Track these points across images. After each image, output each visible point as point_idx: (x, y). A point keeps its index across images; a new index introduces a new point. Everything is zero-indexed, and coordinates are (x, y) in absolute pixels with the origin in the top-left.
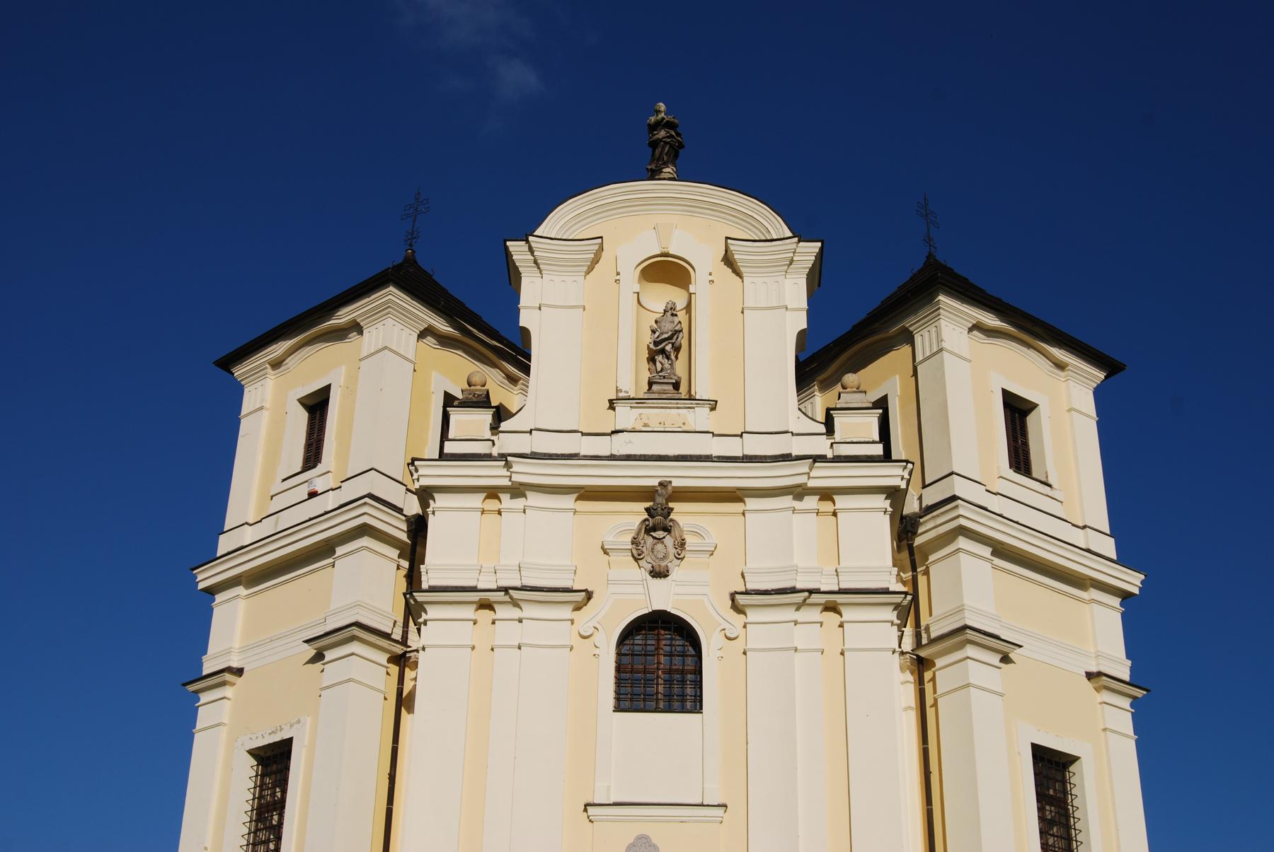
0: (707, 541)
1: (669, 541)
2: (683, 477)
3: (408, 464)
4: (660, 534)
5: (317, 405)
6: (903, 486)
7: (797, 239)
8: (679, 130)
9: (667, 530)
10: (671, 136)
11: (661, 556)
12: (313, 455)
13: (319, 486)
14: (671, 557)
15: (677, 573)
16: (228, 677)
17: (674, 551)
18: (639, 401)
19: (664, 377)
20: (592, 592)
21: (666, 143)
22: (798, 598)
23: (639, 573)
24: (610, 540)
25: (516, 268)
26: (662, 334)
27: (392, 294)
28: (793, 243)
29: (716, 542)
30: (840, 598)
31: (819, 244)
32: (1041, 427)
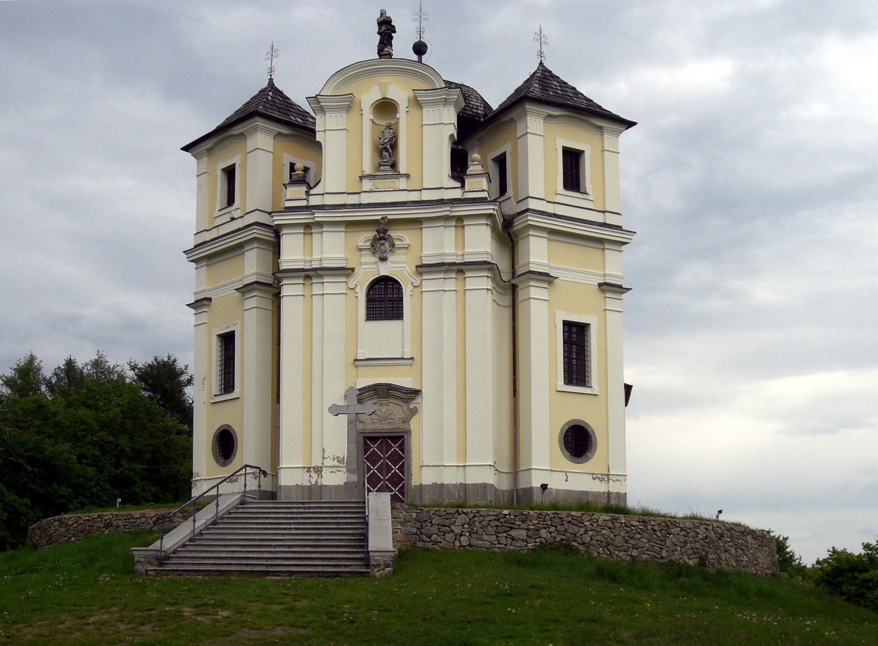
0: (405, 243)
1: (387, 245)
2: (393, 214)
4: (382, 242)
5: (230, 173)
8: (392, 24)
10: (389, 29)
12: (231, 200)
13: (236, 214)
14: (388, 251)
15: (391, 258)
16: (205, 302)
17: (390, 248)
19: (386, 162)
21: (385, 33)
22: (445, 268)
23: (373, 259)
24: (361, 244)
26: (384, 140)
27: (259, 122)
30: (463, 267)
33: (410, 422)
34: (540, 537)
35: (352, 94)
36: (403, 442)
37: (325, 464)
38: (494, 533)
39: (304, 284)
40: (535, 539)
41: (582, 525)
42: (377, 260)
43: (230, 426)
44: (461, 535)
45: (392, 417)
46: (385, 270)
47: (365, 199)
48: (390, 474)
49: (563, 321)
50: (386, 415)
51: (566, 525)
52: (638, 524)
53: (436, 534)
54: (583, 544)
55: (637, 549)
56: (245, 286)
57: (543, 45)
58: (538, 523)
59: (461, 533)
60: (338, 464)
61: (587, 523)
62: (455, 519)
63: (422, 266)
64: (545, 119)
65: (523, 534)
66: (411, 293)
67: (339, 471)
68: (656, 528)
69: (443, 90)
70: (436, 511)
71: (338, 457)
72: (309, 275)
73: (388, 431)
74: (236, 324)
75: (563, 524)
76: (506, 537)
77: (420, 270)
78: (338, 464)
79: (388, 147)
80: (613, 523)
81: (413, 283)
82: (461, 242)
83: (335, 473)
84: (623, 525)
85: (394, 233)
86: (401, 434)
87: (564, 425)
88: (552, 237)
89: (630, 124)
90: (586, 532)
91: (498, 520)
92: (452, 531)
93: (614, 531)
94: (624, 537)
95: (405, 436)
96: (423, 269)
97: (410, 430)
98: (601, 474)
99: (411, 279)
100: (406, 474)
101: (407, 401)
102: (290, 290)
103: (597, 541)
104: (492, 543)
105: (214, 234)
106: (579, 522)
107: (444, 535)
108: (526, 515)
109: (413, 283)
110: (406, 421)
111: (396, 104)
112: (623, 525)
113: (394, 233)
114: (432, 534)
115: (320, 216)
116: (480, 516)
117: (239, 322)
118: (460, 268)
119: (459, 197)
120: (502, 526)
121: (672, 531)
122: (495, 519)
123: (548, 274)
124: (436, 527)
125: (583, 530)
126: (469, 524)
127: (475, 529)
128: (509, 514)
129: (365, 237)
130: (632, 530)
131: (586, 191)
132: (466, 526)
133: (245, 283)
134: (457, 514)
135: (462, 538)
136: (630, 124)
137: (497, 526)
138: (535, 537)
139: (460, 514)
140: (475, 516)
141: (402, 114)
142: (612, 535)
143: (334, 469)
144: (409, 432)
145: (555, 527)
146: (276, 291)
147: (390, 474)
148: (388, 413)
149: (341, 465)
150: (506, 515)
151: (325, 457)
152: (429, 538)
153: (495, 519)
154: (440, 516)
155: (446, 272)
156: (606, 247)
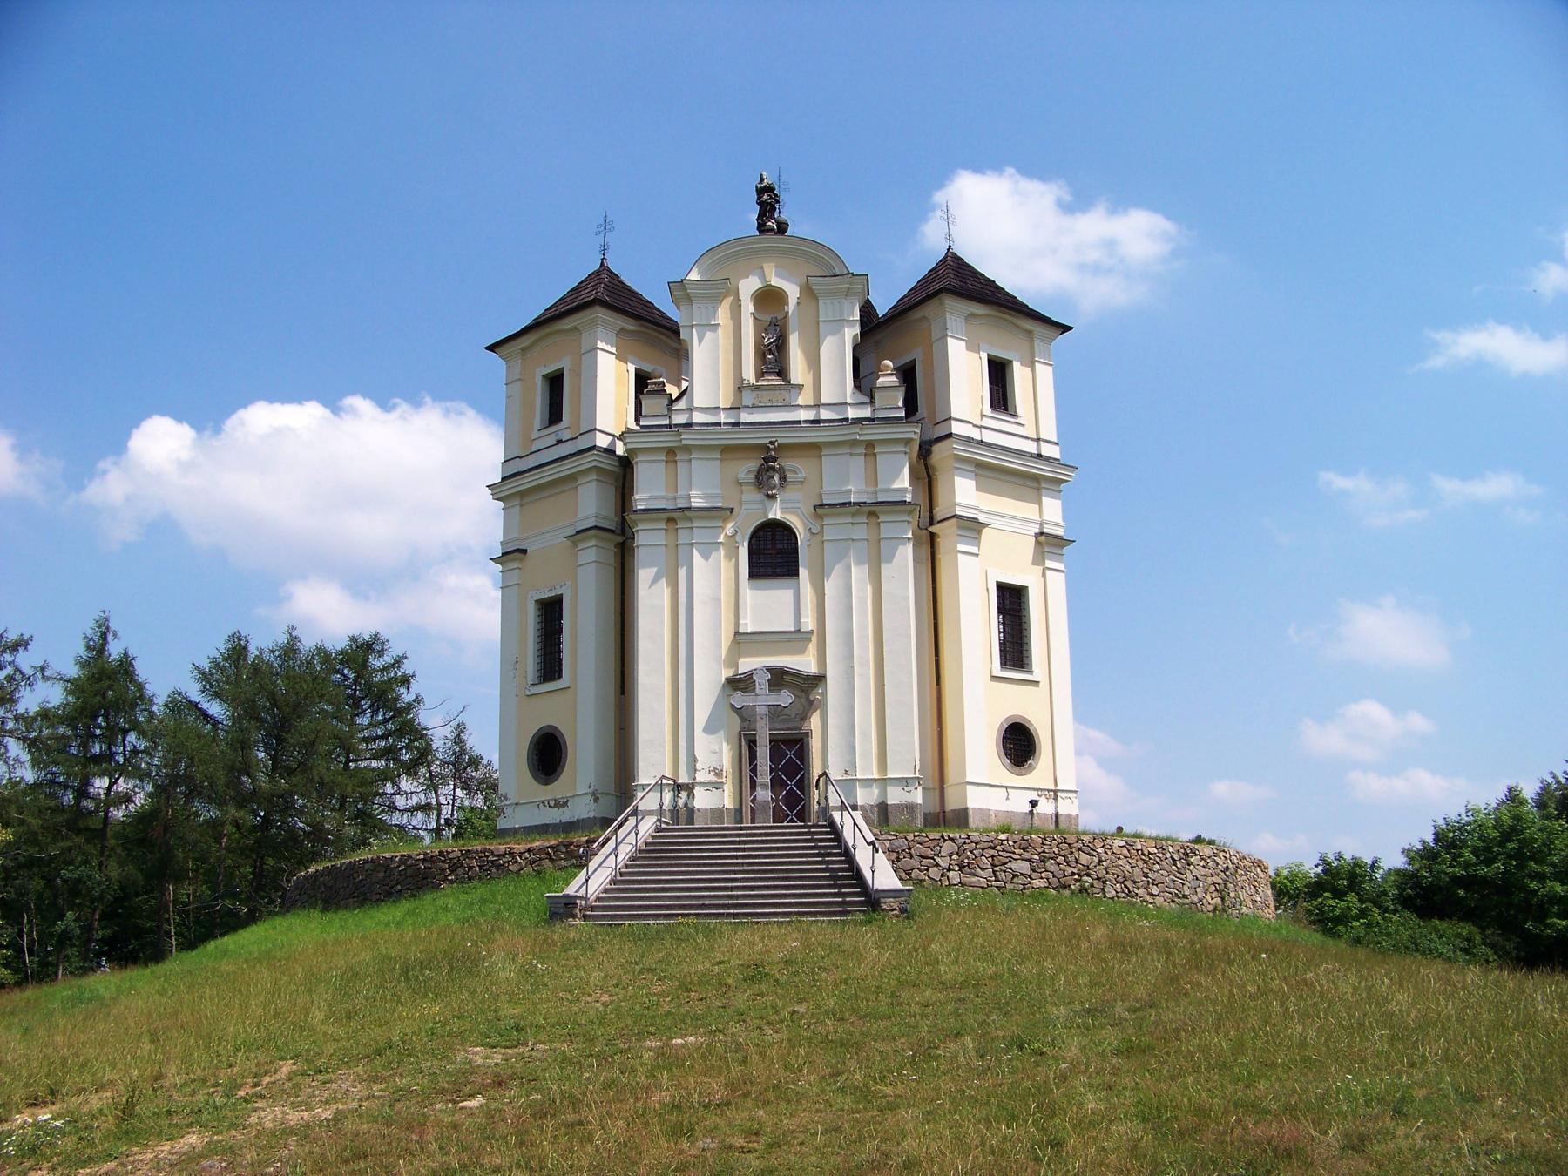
2: (784, 437)
19: (771, 368)
24: (742, 476)
26: (769, 339)
27: (600, 313)
34: (1046, 871)
35: (728, 279)
38: (990, 866)
39: (666, 530)
40: (1041, 873)
41: (1095, 853)
43: (555, 728)
44: (949, 870)
46: (776, 513)
47: (746, 417)
49: (997, 582)
51: (1076, 854)
52: (1156, 851)
53: (918, 869)
54: (1098, 879)
55: (1157, 885)
56: (578, 532)
57: (951, 225)
58: (1044, 852)
59: (949, 867)
61: (1099, 850)
62: (939, 848)
63: (822, 506)
64: (966, 319)
65: (1024, 867)
68: (1175, 856)
70: (915, 836)
72: (674, 516)
74: (565, 584)
75: (1072, 853)
76: (1005, 872)
80: (1129, 851)
82: (873, 477)
84: (1140, 852)
85: (785, 462)
88: (980, 472)
89: (1066, 329)
90: (1101, 861)
91: (994, 848)
92: (937, 865)
93: (1130, 861)
94: (1142, 869)
95: (805, 739)
96: (822, 509)
98: (1049, 791)
102: (647, 538)
103: (1113, 874)
104: (988, 881)
105: (531, 462)
106: (1092, 849)
107: (927, 870)
108: (1027, 841)
109: (810, 529)
110: (804, 717)
112: (1140, 852)
113: (785, 462)
114: (912, 870)
115: (688, 438)
116: (972, 842)
117: (569, 583)
118: (873, 510)
119: (869, 415)
120: (1000, 855)
121: (1192, 860)
122: (990, 847)
123: (977, 519)
124: (916, 858)
125: (1096, 860)
126: (957, 854)
127: (966, 861)
128: (1007, 840)
129: (746, 468)
130: (1150, 859)
131: (1016, 412)
132: (955, 857)
133: (578, 529)
134: (942, 840)
135: (951, 874)
136: (1066, 329)
137: (993, 856)
138: (1040, 871)
139: (945, 840)
140: (965, 843)
142: (1128, 867)
145: (1064, 856)
146: (620, 539)
150: (1002, 841)
152: (909, 875)
153: (990, 847)
154: (921, 844)
155: (853, 515)
156: (1043, 485)
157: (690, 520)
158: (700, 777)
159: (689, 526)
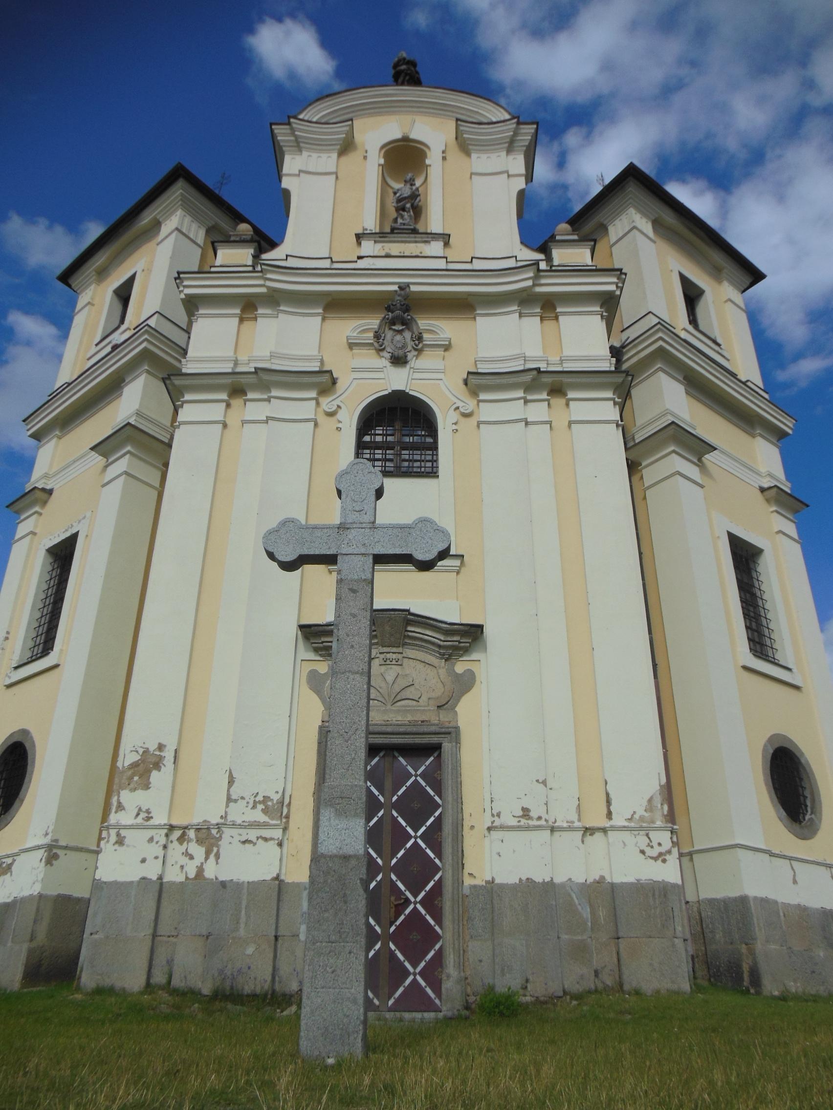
0: (442, 336)
1: (407, 335)
3: (176, 279)
6: (618, 293)
7: (515, 120)
9: (404, 323)
11: (399, 345)
14: (410, 348)
17: (413, 343)
18: (380, 236)
19: (404, 224)
20: (337, 379)
22: (528, 377)
25: (281, 147)
28: (513, 124)
29: (449, 337)
30: (566, 379)
31: (535, 126)
32: (707, 306)
33: (457, 709)
36: (438, 764)
37: (230, 818)
42: (383, 362)
45: (407, 693)
48: (402, 852)
50: (397, 688)
60: (263, 818)
66: (454, 427)
67: (266, 840)
69: (508, 123)
71: (266, 799)
73: (402, 729)
74: (84, 518)
77: (473, 380)
78: (263, 818)
79: (408, 205)
81: (458, 408)
83: (255, 844)
86: (434, 739)
87: (765, 746)
95: (446, 746)
97: (457, 729)
99: (456, 400)
100: (448, 849)
101: (451, 653)
110: (447, 704)
111: (422, 147)
113: (423, 323)
117: (88, 514)
141: (433, 159)
143: (252, 834)
144: (453, 733)
147: (402, 852)
148: (402, 683)
149: (274, 822)
151: (234, 797)
155: (529, 388)
157: (265, 387)
158: (240, 813)
159: (265, 397)
